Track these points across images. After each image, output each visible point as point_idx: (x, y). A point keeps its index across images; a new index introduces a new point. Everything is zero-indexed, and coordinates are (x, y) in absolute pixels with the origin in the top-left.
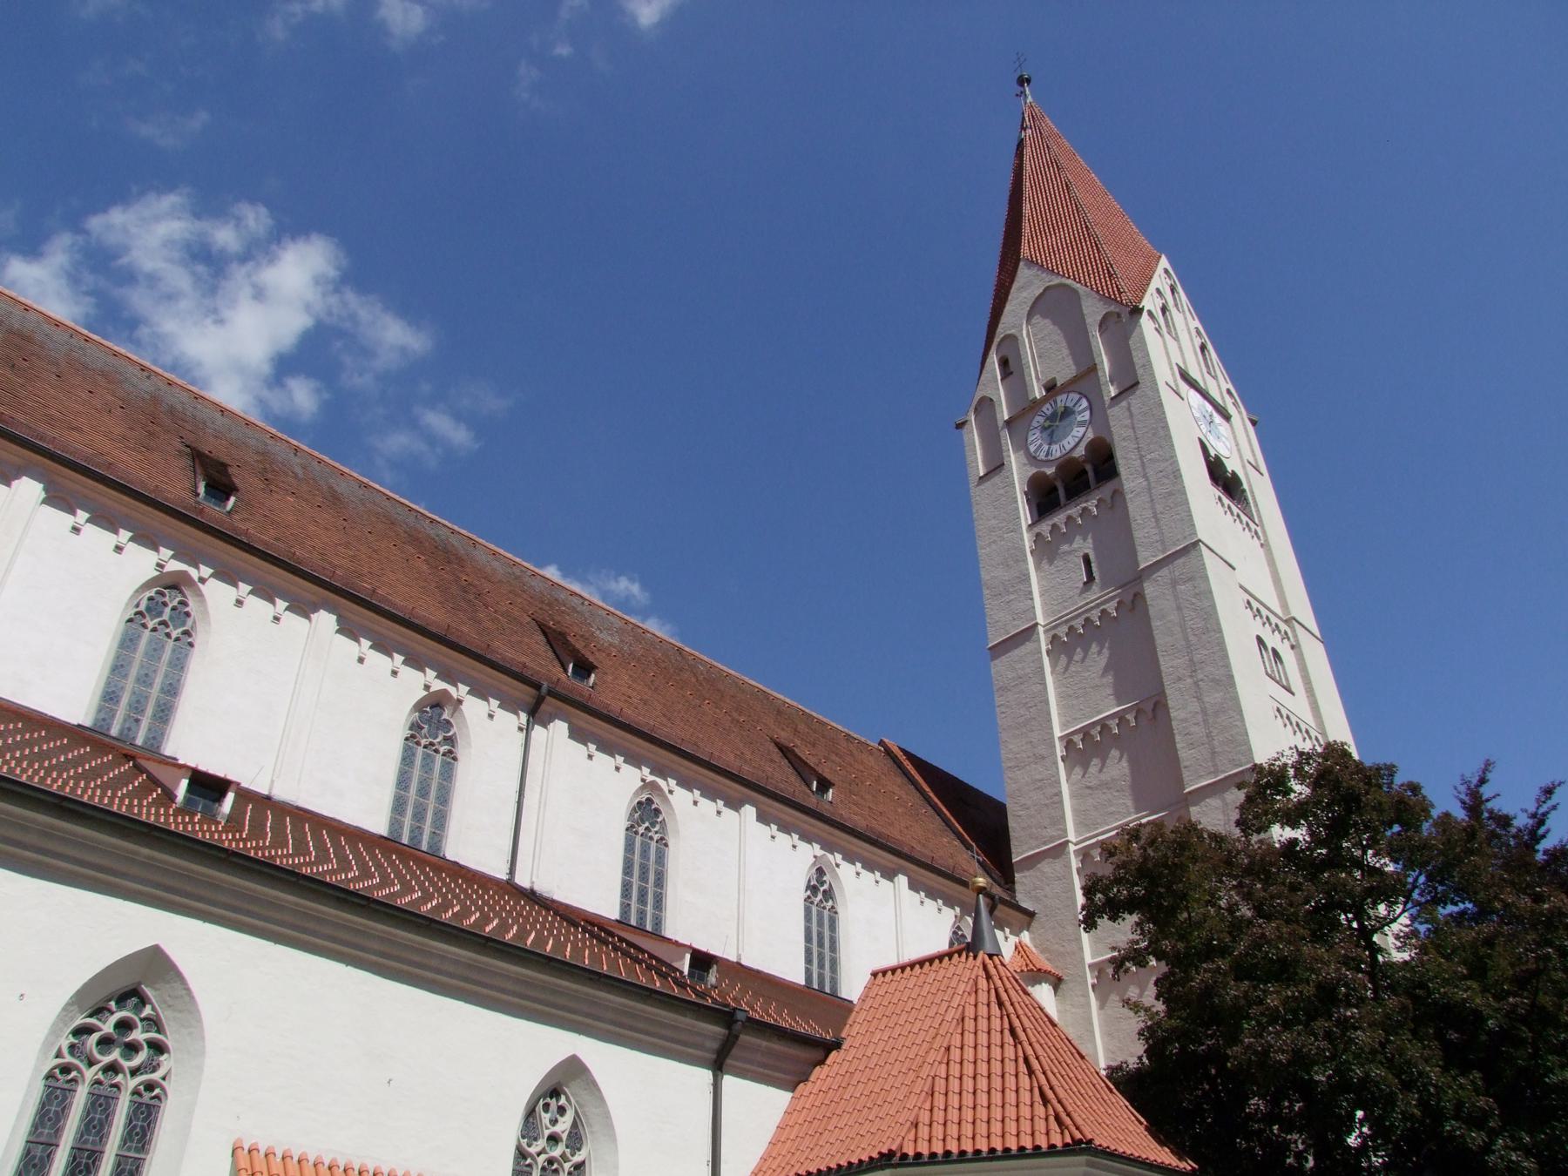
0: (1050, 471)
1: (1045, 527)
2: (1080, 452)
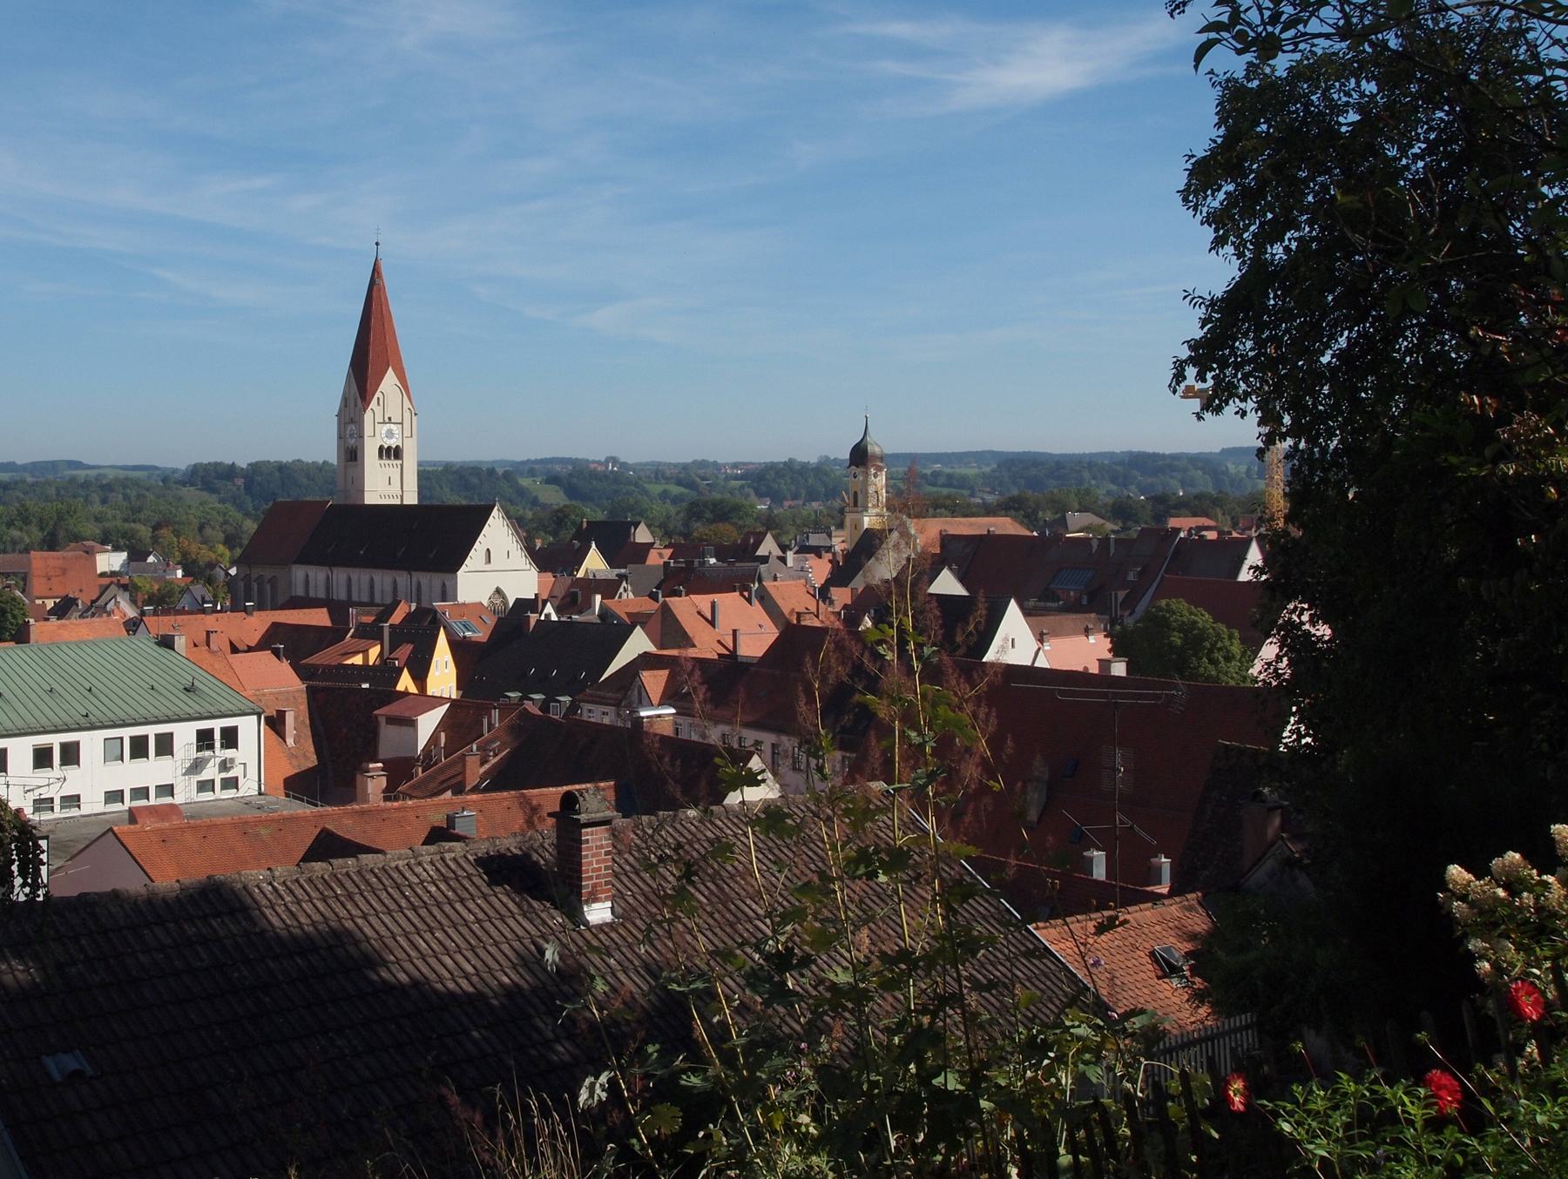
1: (382, 462)
2: (394, 446)
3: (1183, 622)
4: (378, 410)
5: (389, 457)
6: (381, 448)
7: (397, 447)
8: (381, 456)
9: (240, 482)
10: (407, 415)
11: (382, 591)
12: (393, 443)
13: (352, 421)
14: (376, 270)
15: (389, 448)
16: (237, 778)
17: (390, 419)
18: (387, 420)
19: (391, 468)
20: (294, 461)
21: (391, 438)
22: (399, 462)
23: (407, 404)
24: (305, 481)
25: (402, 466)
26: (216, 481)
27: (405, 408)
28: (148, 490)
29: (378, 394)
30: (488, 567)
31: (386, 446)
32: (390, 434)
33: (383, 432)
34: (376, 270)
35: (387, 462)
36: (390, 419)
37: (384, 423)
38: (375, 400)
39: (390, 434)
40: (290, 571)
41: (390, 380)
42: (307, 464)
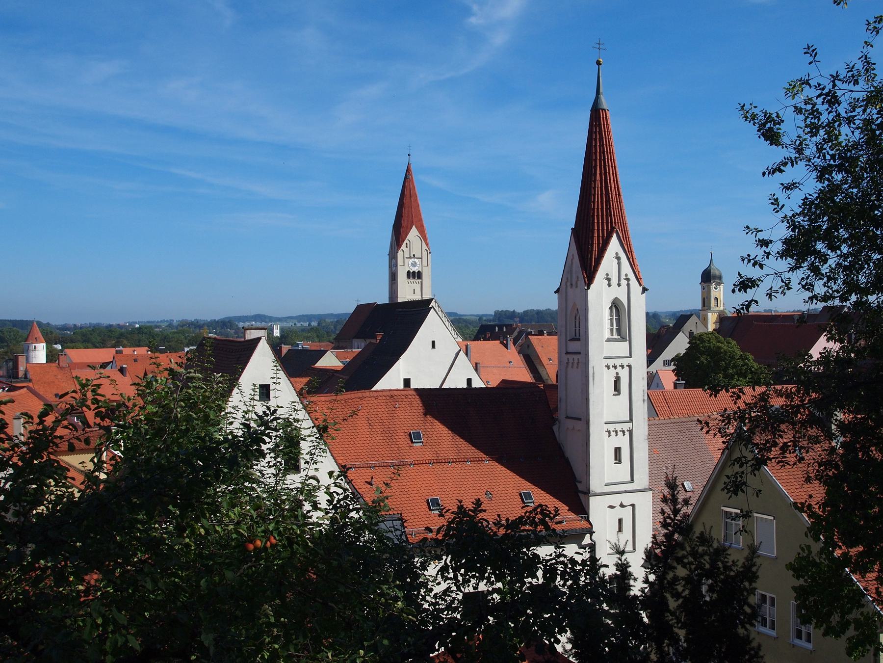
1: (409, 280)
2: (417, 271)
4: (407, 251)
5: (414, 278)
6: (409, 272)
7: (419, 271)
8: (408, 277)
10: (425, 253)
12: (416, 269)
13: (394, 258)
14: (408, 171)
15: (414, 272)
17: (414, 255)
18: (412, 256)
19: (415, 284)
20: (546, 310)
21: (415, 266)
22: (420, 281)
24: (550, 319)
25: (422, 282)
26: (505, 320)
27: (424, 249)
28: (470, 324)
29: (406, 241)
31: (412, 271)
32: (414, 264)
34: (408, 171)
35: (414, 280)
36: (414, 255)
37: (410, 258)
38: (404, 244)
39: (414, 264)
40: (352, 342)
41: (414, 233)
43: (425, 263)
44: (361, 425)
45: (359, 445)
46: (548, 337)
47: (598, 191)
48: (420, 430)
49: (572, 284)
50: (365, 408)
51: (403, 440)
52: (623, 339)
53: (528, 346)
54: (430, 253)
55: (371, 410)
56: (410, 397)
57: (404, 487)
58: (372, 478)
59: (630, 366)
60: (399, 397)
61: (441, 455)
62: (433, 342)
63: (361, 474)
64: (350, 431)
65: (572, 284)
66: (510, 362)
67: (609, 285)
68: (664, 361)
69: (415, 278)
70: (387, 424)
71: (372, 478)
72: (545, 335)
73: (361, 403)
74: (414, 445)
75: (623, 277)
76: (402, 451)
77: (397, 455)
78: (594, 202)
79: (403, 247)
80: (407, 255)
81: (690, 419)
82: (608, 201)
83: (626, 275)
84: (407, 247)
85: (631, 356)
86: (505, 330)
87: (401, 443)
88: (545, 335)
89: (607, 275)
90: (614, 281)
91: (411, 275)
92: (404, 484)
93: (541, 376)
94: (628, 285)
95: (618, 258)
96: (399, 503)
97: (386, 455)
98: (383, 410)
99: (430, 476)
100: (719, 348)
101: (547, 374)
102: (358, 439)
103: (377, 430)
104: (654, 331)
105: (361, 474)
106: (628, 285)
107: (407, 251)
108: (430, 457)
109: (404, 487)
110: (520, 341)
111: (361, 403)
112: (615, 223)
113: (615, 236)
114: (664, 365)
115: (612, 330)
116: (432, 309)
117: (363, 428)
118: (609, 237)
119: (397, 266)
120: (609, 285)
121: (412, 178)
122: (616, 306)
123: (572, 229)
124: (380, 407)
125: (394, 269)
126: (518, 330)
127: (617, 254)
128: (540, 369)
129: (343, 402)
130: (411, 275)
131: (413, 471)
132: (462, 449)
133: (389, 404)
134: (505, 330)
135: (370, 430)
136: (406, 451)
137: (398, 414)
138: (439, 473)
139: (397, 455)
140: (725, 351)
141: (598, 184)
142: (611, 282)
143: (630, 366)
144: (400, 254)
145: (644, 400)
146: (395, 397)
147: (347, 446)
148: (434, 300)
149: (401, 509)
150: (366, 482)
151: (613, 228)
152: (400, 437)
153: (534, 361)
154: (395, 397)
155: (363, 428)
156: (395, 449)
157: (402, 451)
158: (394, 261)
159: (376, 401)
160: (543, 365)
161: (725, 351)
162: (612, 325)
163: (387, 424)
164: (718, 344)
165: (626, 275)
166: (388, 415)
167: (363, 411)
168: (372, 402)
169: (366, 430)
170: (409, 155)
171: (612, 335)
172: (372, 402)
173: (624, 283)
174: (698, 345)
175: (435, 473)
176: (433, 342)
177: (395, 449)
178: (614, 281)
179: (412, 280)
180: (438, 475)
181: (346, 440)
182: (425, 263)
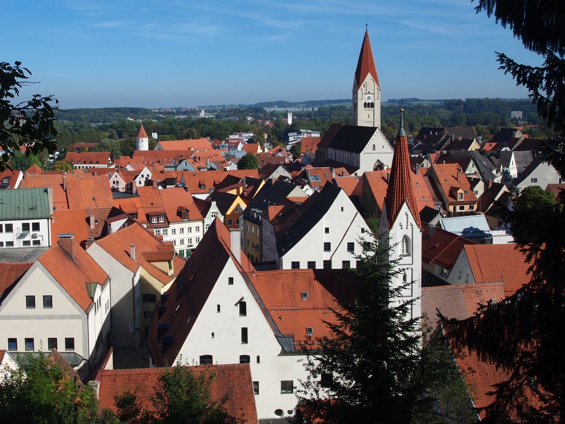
0: (367, 103)
1: (366, 109)
2: (371, 103)
3: (534, 197)
4: (364, 89)
5: (369, 107)
6: (365, 103)
7: (372, 103)
9: (462, 106)
10: (376, 91)
11: (345, 159)
12: (370, 101)
15: (369, 103)
16: (39, 241)
17: (369, 92)
18: (368, 93)
19: (370, 111)
20: (485, 99)
23: (376, 86)
24: (487, 106)
25: (374, 110)
26: (453, 106)
30: (374, 152)
31: (367, 103)
32: (369, 98)
33: (366, 97)
35: (369, 109)
36: (369, 92)
37: (367, 94)
38: (362, 85)
39: (369, 98)
41: (369, 77)
42: (490, 99)
43: (376, 97)
44: (279, 288)
45: (277, 298)
46: (446, 164)
47: (398, 180)
48: (307, 291)
49: (384, 225)
50: (282, 279)
51: (298, 296)
52: (409, 255)
53: (432, 171)
54: (380, 90)
55: (284, 280)
56: (304, 273)
57: (296, 321)
58: (281, 316)
59: (412, 269)
60: (299, 274)
61: (316, 305)
62: (342, 208)
63: (277, 314)
64: (273, 291)
65: (384, 225)
66: (417, 183)
67: (401, 228)
68: (532, 179)
69: (369, 107)
70: (291, 288)
71: (281, 316)
72: (444, 163)
73: (280, 276)
74: (303, 299)
75: (409, 224)
76: (297, 302)
77: (295, 304)
78: (395, 185)
79: (362, 87)
80: (364, 92)
81: (458, 287)
82: (402, 185)
83: (411, 223)
84: (364, 86)
85: (412, 264)
86: (436, 134)
87: (297, 298)
88: (444, 163)
89: (400, 223)
90: (404, 226)
91: (366, 105)
92: (296, 319)
93: (439, 191)
94: (412, 228)
95: (407, 215)
96: (293, 329)
97: (289, 304)
98: (290, 280)
99: (309, 316)
100: (541, 198)
101: (443, 190)
102: (277, 295)
103: (286, 291)
104: (518, 167)
105: (277, 314)
106: (412, 228)
107: (364, 89)
108: (311, 307)
109: (296, 321)
110: (446, 143)
111: (280, 276)
112: (406, 197)
113: (405, 204)
114: (532, 182)
115: (403, 250)
116: (342, 190)
117: (280, 289)
118: (402, 204)
119: (357, 99)
120: (401, 228)
121: (369, 40)
122: (406, 238)
123: (384, 197)
124: (289, 278)
125: (356, 101)
126: (445, 135)
127: (406, 213)
128: (439, 187)
129: (271, 275)
130: (366, 105)
131: (301, 313)
132: (327, 302)
133: (293, 277)
134: (436, 134)
135: (283, 291)
136: (299, 302)
137: (298, 283)
138: (314, 314)
139: (295, 304)
140: (544, 200)
141: (398, 176)
142: (402, 227)
143: (412, 269)
144: (359, 92)
145: (419, 286)
146: (297, 274)
147: (271, 299)
148: (378, 128)
149: (293, 332)
150: (279, 317)
151: (404, 200)
152: (297, 295)
153: (435, 181)
154: (297, 274)
155: (280, 289)
156: (294, 301)
157: (297, 302)
158: (355, 95)
159: (287, 276)
160: (441, 184)
161: (544, 200)
162: (403, 248)
163: (291, 288)
164: (540, 195)
165: (411, 223)
166: (292, 283)
167: (281, 280)
168: (285, 276)
169: (281, 291)
170: (367, 25)
171: (403, 253)
172: (285, 276)
173: (410, 227)
174: (527, 195)
175: (312, 314)
176: (342, 208)
177: (294, 301)
178: (404, 226)
179: (367, 109)
180: (313, 316)
181: (271, 296)
182: (376, 97)
